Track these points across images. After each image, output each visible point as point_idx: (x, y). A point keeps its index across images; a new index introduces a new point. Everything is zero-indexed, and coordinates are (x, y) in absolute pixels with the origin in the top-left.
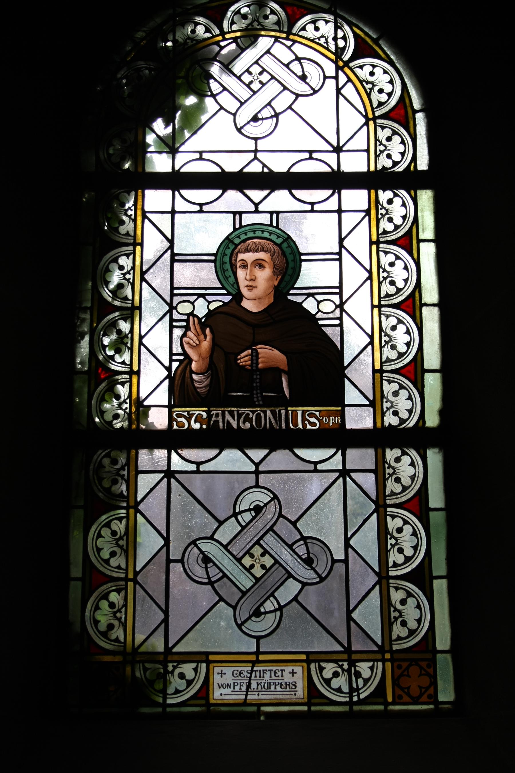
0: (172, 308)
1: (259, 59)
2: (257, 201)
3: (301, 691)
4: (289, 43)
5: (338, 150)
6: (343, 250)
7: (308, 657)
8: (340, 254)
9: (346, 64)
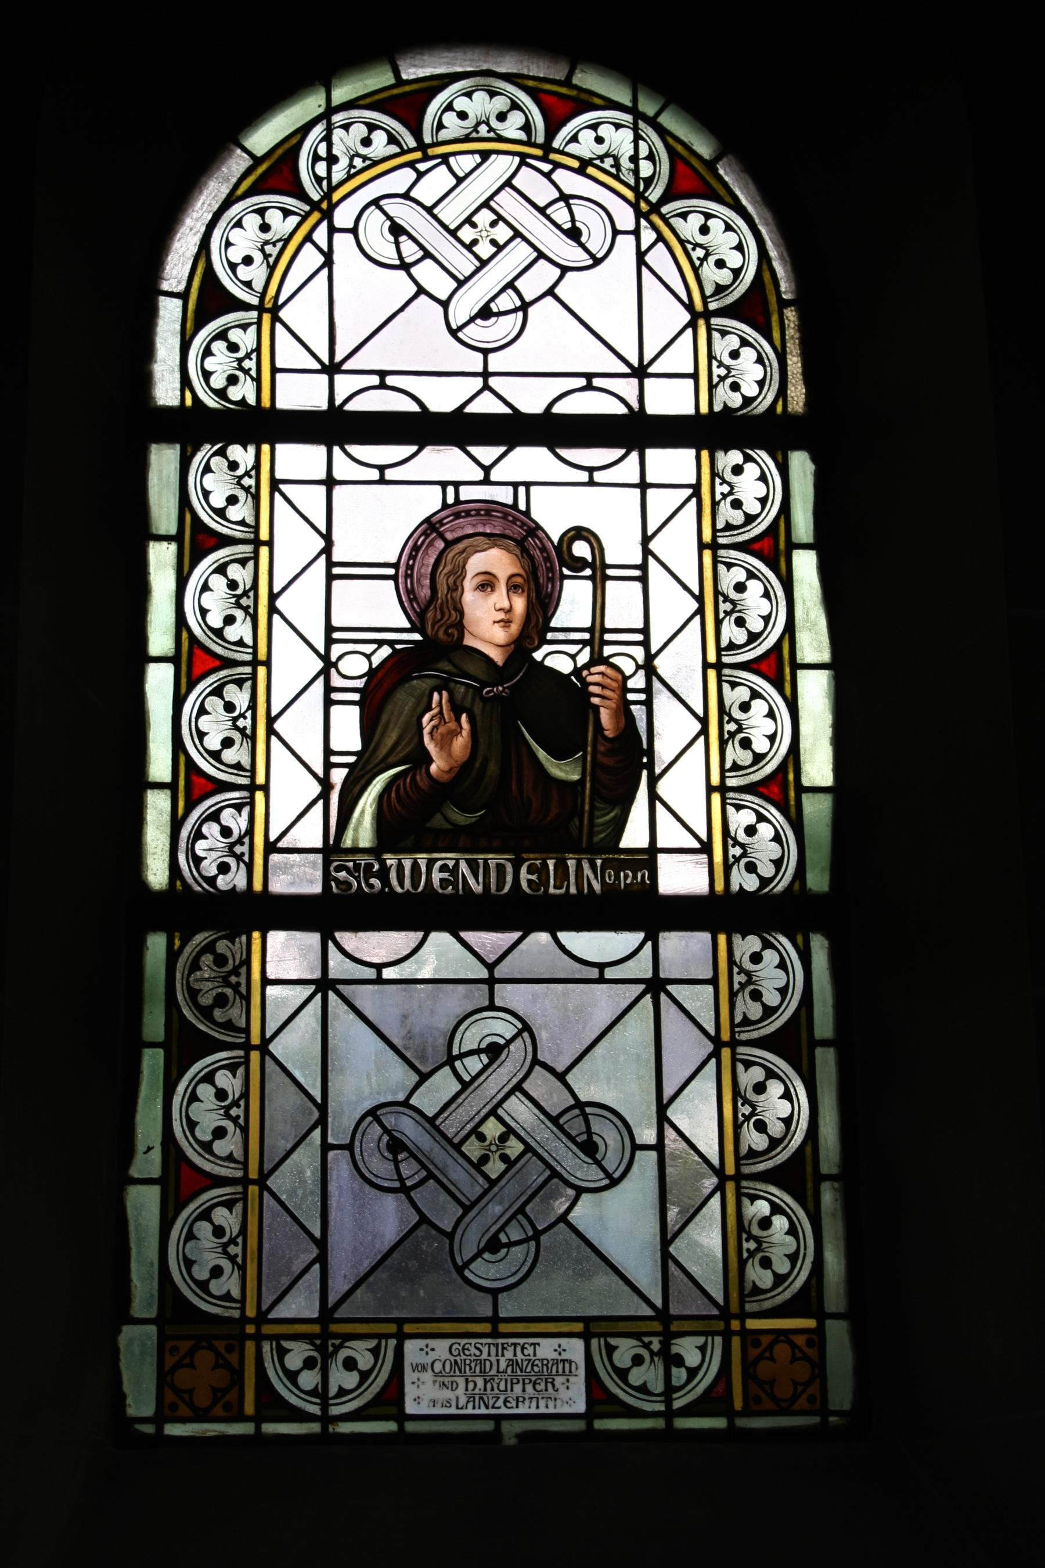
0: (329, 665)
1: (491, 197)
2: (487, 462)
3: (574, 1398)
4: (546, 167)
5: (640, 372)
6: (650, 559)
7: (586, 1327)
8: (644, 567)
9: (655, 208)
